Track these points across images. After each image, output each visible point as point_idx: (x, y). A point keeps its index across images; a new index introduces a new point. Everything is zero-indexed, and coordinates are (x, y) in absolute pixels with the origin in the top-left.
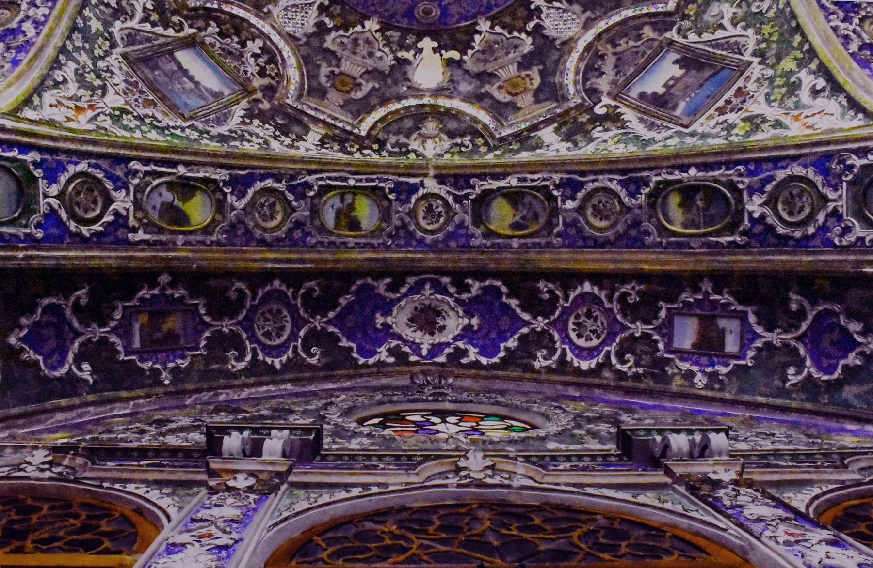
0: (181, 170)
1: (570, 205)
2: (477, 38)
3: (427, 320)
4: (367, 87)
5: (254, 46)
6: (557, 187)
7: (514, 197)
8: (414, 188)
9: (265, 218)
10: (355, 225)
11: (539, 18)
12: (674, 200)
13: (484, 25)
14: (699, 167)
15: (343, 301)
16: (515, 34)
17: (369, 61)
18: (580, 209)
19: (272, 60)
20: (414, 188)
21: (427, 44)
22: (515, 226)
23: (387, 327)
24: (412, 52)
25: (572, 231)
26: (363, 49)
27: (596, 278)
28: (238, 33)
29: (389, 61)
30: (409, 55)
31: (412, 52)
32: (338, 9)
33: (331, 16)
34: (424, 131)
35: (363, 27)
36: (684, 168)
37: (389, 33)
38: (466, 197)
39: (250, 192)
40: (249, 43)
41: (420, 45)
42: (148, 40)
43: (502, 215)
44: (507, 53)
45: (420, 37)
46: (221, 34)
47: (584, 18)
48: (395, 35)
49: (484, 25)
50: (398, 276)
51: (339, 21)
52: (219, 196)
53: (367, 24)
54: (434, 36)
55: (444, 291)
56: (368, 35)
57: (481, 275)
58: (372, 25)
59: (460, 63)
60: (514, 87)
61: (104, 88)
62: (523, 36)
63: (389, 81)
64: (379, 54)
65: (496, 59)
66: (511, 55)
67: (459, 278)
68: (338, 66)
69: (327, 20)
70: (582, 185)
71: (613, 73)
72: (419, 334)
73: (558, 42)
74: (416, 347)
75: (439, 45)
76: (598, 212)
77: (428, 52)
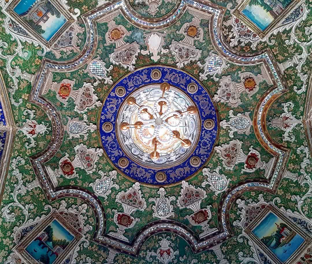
2: (134, 63)
4: (182, 31)
5: (234, 42)
11: (108, 72)
13: (131, 68)
16: (117, 64)
17: (181, 46)
19: (226, 37)
21: (155, 58)
24: (162, 53)
26: (184, 52)
28: (242, 48)
29: (172, 47)
31: (162, 53)
33: (198, 67)
34: (156, 6)
35: (184, 64)
37: (173, 62)
40: (236, 44)
41: (159, 57)
42: (288, 19)
44: (121, 53)
45: (159, 62)
46: (250, 44)
48: (170, 61)
49: (131, 68)
53: (182, 65)
54: (153, 63)
56: (182, 60)
58: (180, 65)
59: (142, 48)
60: (117, 35)
62: (114, 62)
63: (172, 36)
64: (177, 51)
65: (125, 51)
66: (119, 52)
68: (195, 41)
69: (200, 65)
71: (73, 35)
73: (99, 58)
75: (150, 57)
77: (155, 54)
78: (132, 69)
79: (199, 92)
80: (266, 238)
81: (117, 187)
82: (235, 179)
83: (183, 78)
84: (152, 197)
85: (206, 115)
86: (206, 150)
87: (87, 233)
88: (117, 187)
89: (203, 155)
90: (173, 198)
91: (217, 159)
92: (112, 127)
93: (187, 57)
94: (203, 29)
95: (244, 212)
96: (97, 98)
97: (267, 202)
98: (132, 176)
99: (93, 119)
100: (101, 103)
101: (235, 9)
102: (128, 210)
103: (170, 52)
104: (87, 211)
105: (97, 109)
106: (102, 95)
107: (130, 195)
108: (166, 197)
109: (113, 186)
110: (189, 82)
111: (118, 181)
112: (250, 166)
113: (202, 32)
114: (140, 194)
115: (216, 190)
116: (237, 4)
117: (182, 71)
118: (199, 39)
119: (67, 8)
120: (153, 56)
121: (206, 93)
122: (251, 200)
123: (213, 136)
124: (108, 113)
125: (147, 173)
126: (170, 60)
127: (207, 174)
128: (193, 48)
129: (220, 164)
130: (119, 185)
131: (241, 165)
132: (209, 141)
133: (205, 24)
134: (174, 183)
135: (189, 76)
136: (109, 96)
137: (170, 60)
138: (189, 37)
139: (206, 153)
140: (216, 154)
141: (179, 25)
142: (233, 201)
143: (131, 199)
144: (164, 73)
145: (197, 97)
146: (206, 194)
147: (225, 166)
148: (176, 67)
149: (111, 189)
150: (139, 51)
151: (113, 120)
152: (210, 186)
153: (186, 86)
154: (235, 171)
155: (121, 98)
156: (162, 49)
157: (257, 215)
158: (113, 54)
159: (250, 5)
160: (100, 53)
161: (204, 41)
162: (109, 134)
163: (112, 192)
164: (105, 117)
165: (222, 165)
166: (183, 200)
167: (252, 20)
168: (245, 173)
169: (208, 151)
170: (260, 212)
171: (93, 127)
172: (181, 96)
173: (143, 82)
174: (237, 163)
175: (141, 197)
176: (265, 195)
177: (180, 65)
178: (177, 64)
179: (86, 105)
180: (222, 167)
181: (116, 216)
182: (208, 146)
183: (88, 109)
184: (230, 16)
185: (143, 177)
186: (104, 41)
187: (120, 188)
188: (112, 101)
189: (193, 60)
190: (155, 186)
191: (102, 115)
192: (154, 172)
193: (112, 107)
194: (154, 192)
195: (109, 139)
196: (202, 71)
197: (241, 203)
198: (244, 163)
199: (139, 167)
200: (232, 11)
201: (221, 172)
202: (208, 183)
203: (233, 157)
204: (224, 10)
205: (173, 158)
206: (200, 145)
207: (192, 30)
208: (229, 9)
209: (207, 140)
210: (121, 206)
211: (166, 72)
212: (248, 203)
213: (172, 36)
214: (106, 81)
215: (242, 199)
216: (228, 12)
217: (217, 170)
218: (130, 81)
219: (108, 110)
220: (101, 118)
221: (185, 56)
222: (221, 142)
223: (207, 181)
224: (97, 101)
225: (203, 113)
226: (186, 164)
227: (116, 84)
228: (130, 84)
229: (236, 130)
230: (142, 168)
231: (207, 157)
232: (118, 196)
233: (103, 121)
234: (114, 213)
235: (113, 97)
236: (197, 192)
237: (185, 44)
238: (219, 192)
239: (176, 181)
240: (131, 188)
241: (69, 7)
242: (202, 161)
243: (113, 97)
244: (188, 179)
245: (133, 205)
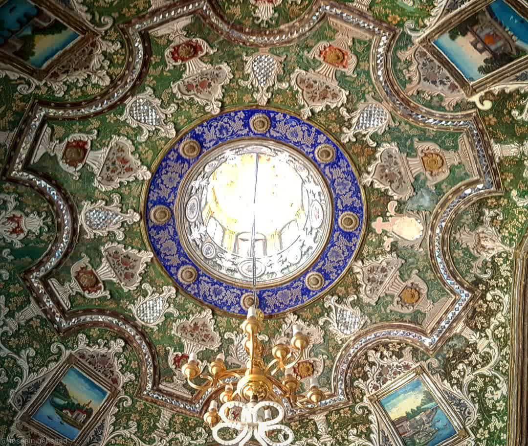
2: (376, 186)
4: (415, 278)
11: (365, 136)
17: (390, 274)
21: (378, 225)
24: (385, 238)
26: (378, 276)
29: (392, 257)
30: (387, 242)
31: (385, 238)
32: (341, 290)
33: (347, 294)
35: (358, 273)
37: (365, 254)
47: (371, 101)
51: (351, 289)
53: (356, 270)
54: (369, 220)
58: (358, 267)
63: (411, 260)
64: (384, 264)
68: (393, 297)
69: (351, 299)
75: (381, 216)
77: (387, 226)
78: (365, 181)
79: (306, 291)
80: (66, 390)
81: (143, 138)
82: (156, 337)
83: (335, 267)
84: (122, 199)
85: (266, 298)
86: (207, 294)
87: (50, 88)
88: (143, 138)
89: (198, 288)
90: (120, 237)
91: (191, 311)
92: (262, 130)
93: (369, 280)
94: (409, 314)
95: (103, 351)
96: (317, 110)
97: (123, 387)
98: (164, 164)
99: (278, 100)
100: (306, 117)
101: (427, 369)
102: (96, 159)
103: (383, 253)
104: (96, 85)
105: (297, 107)
106: (322, 120)
107: (125, 161)
108: (122, 223)
109: (145, 131)
110: (326, 276)
111: (154, 139)
112: (179, 361)
113: (405, 311)
114: (128, 179)
115: (137, 306)
116: (433, 375)
117: (347, 268)
118: (395, 303)
119: (496, 88)
120: (384, 221)
121: (303, 301)
122: (124, 362)
123: (229, 307)
124: (288, 126)
125: (169, 190)
126: (371, 249)
127: (166, 294)
128: (381, 292)
129: (182, 314)
130: (146, 142)
131: (181, 347)
132: (222, 300)
133: (417, 318)
134: (150, 237)
135: (336, 278)
136: (318, 132)
137: (371, 249)
138: (401, 289)
139: (201, 293)
140: (199, 309)
141: (427, 275)
142: (120, 335)
143: (117, 164)
144: (349, 236)
145: (297, 287)
146: (130, 290)
147: (178, 322)
148: (356, 260)
149: (139, 127)
150: (395, 198)
151: (273, 133)
152: (145, 297)
153: (320, 270)
154: (171, 338)
155: (313, 152)
156: (392, 240)
157: (99, 371)
158: (397, 149)
159: (425, 392)
160: (400, 127)
161: (388, 311)
162: (247, 125)
163: (134, 129)
164: (279, 121)
165: (180, 317)
166: (116, 252)
167: (404, 389)
168: (167, 353)
169: (205, 297)
170: (106, 376)
171: (262, 98)
172: (304, 258)
173: (338, 196)
174: (183, 340)
175: (123, 180)
176: (133, 383)
177: (358, 267)
178: (360, 262)
179: (305, 89)
180: (178, 317)
181: (84, 137)
182: (213, 297)
183: (297, 91)
184: (417, 359)
185: (162, 183)
186: (423, 138)
187: (141, 144)
188: (309, 135)
189: (362, 290)
190: (143, 205)
191: (285, 116)
192: (170, 203)
193: (297, 135)
194: (132, 202)
195: (237, 125)
196: (340, 301)
197: (117, 345)
198: (183, 350)
199: (181, 176)
200: (425, 364)
201: (168, 316)
202: (150, 294)
203: (192, 335)
204: (431, 353)
205: (195, 235)
206: (217, 283)
207: (413, 296)
208: (428, 361)
209: (223, 297)
210: (103, 145)
211: (350, 240)
212: (119, 357)
213: (411, 260)
214: (349, 131)
215: (124, 348)
216: (425, 357)
217: (172, 309)
218: (343, 172)
219: (294, 127)
220: (278, 113)
221: (371, 277)
222: (219, 318)
223: (153, 292)
224: (312, 111)
225: (270, 293)
226: (182, 258)
227: (341, 148)
228: (337, 173)
229: (236, 343)
230: (179, 183)
231: (195, 294)
232: (123, 139)
233: (272, 115)
234: (90, 132)
235: (316, 138)
236: (133, 275)
237: (392, 280)
238: (134, 311)
239: (152, 240)
240: (140, 163)
241: (496, 93)
242: (189, 286)
243: (316, 138)
244: (156, 262)
245: (105, 167)
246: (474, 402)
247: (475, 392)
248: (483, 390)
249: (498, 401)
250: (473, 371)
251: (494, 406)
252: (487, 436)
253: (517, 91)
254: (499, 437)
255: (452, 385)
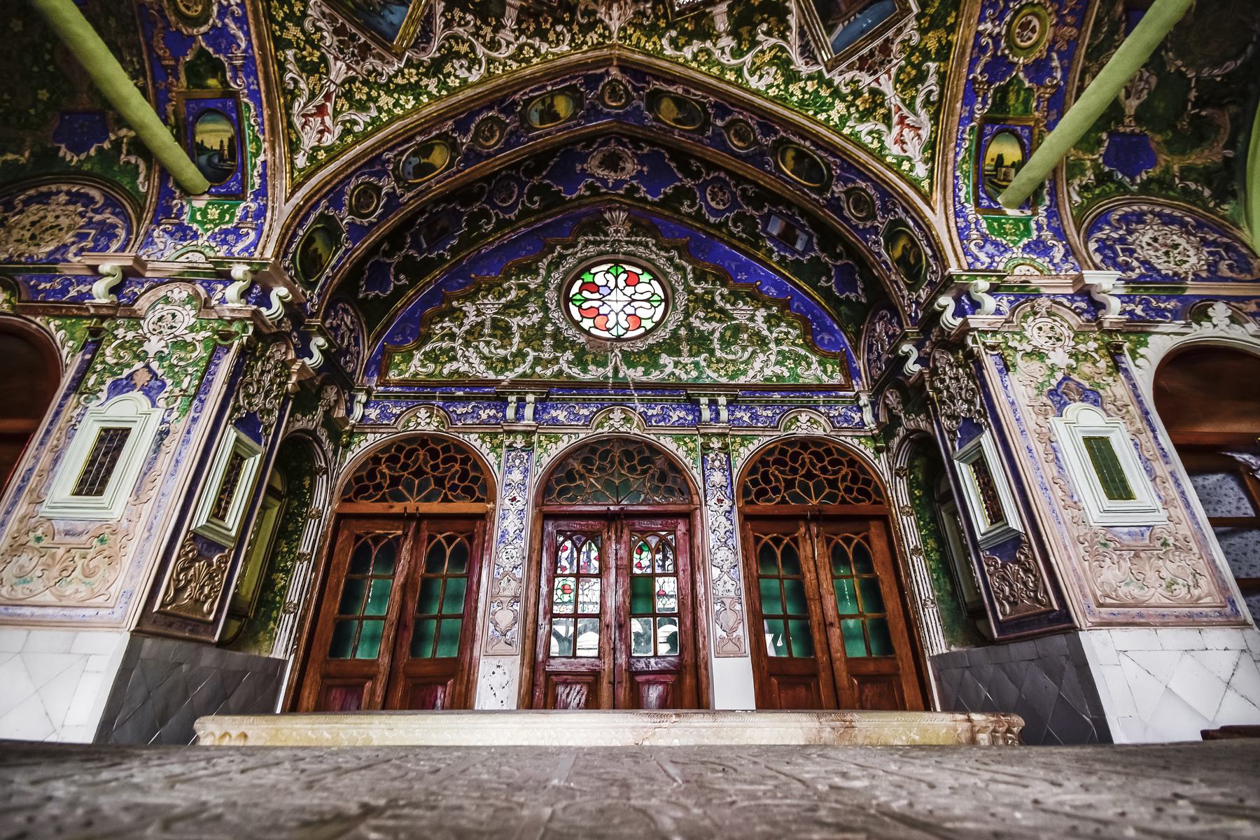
0: (419, 139)
1: (719, 123)
3: (612, 162)
6: (712, 107)
7: (679, 102)
8: (601, 77)
9: (487, 139)
10: (556, 117)
12: (790, 154)
14: (813, 143)
15: (552, 163)
18: (727, 127)
20: (601, 77)
22: (677, 121)
23: (583, 170)
25: (718, 139)
27: (728, 172)
36: (805, 139)
38: (643, 89)
39: (473, 127)
43: (668, 111)
50: (590, 139)
52: (450, 140)
55: (625, 145)
57: (651, 143)
61: (323, 58)
67: (636, 142)
70: (731, 113)
72: (606, 172)
74: (604, 181)
76: (737, 134)
246: (439, 50)
247: (452, 47)
248: (458, 56)
249: (457, 77)
250: (473, 35)
251: (449, 75)
252: (412, 81)
253: (789, 28)
254: (420, 94)
255: (443, 14)
